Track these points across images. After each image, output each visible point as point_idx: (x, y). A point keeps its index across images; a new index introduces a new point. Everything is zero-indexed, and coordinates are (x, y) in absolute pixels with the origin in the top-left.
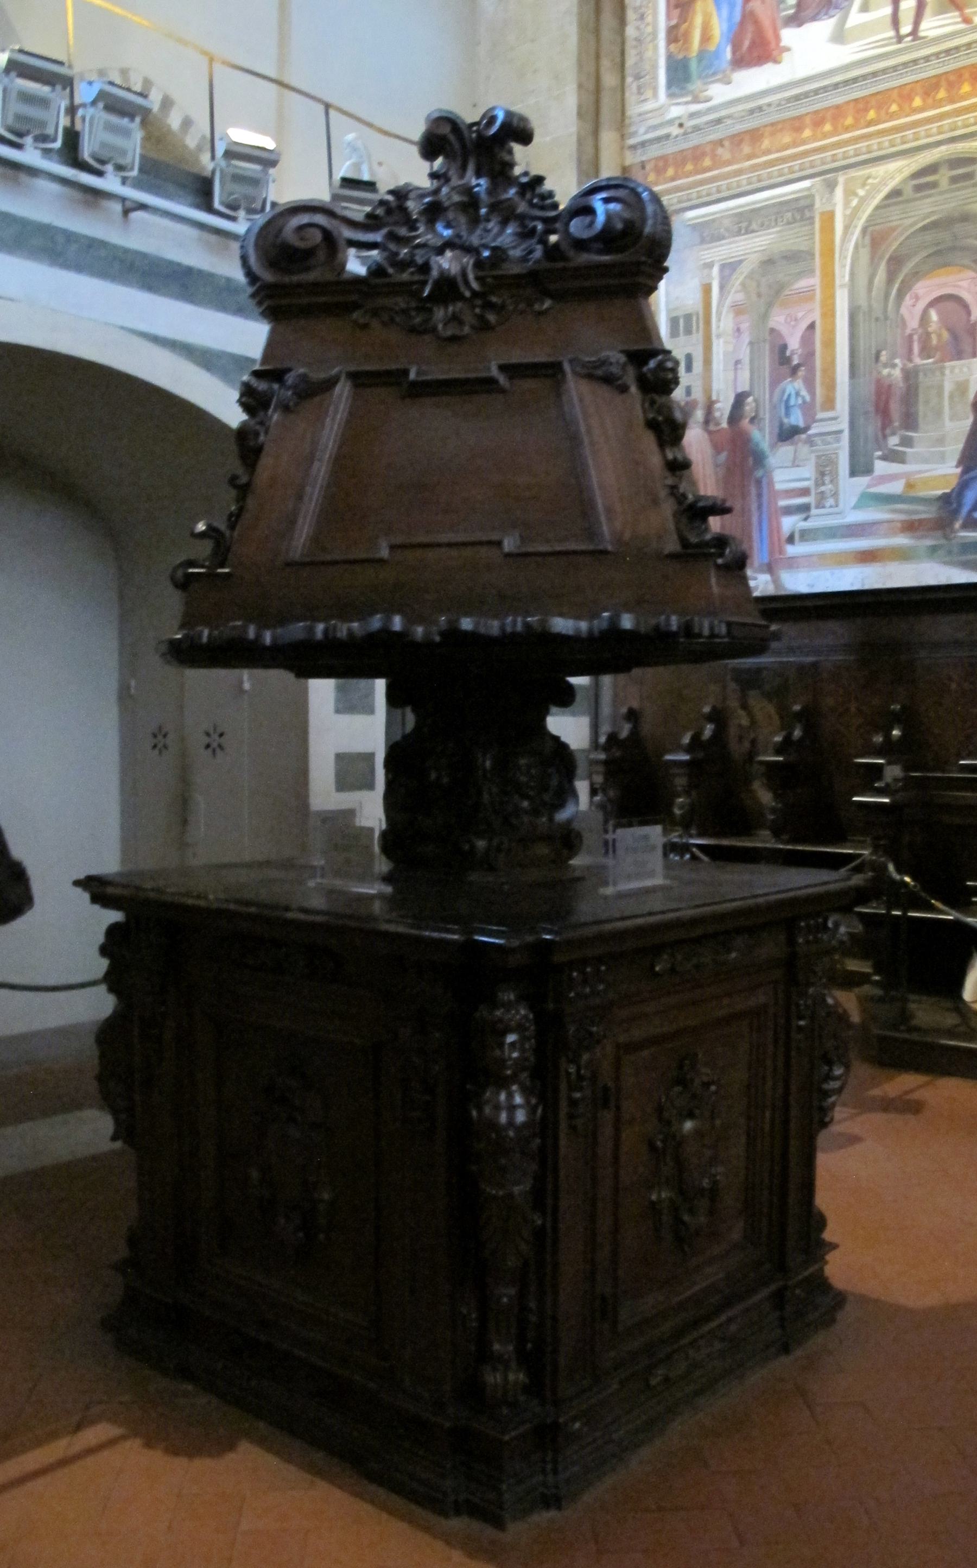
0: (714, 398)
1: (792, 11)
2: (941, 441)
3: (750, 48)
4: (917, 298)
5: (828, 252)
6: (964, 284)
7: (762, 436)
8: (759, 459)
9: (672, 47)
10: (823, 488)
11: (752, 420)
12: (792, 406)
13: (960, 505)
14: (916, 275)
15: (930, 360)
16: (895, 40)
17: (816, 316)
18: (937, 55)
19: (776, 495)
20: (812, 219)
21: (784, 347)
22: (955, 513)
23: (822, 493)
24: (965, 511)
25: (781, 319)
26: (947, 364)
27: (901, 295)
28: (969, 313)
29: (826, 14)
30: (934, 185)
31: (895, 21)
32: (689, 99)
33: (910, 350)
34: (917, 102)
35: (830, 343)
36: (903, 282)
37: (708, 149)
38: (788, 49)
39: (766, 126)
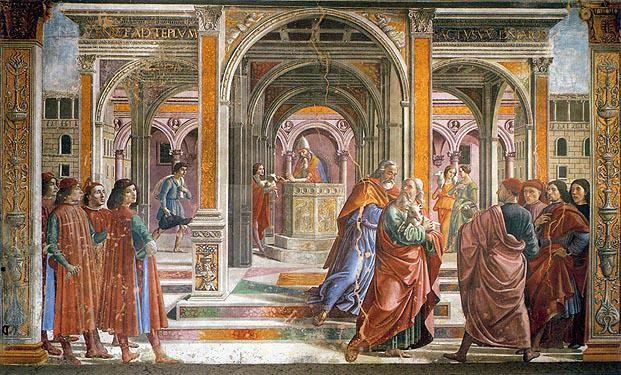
7: (143, 222)
10: (204, 273)
11: (133, 206)
14: (291, 107)
15: (304, 180)
17: (198, 124)
19: (155, 276)
21: (167, 146)
25: (164, 121)
27: (277, 121)
28: (337, 148)
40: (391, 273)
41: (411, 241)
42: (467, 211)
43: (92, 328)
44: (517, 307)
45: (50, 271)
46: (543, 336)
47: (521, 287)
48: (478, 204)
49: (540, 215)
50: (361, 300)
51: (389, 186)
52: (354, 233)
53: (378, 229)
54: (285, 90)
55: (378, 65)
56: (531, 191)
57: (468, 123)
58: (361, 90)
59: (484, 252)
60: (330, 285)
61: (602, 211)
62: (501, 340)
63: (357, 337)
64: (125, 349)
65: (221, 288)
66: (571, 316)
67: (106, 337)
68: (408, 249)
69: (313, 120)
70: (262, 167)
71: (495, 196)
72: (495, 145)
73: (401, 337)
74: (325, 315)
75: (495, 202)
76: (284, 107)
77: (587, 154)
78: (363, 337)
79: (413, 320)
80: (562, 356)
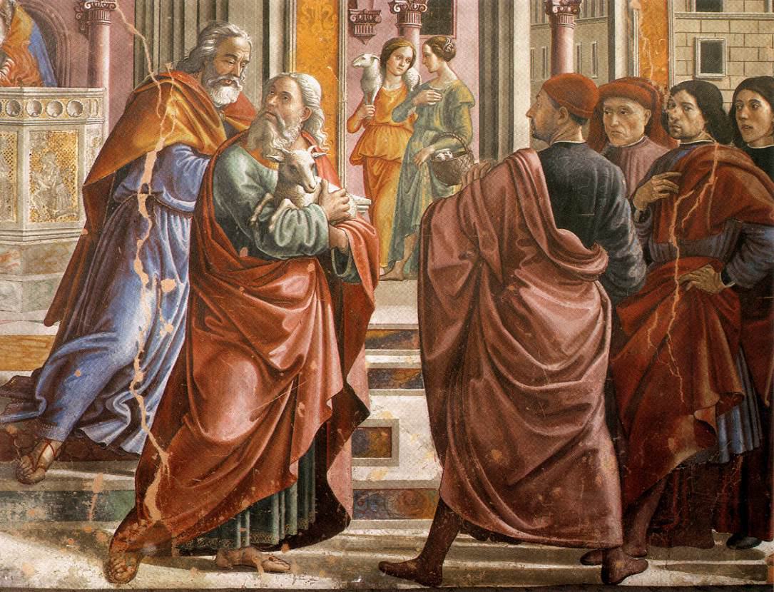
40: (232, 337)
41: (287, 249)
42: (445, 165)
44: (585, 433)
46: (657, 511)
47: (594, 378)
48: (475, 147)
49: (648, 177)
50: (148, 412)
51: (227, 95)
52: (130, 223)
53: (197, 217)
56: (624, 112)
59: (492, 275)
60: (63, 369)
62: (541, 523)
63: (138, 513)
66: (733, 456)
68: (282, 270)
71: (522, 124)
73: (261, 516)
74: (48, 453)
75: (522, 139)
78: (155, 515)
79: (294, 468)
80: (710, 569)
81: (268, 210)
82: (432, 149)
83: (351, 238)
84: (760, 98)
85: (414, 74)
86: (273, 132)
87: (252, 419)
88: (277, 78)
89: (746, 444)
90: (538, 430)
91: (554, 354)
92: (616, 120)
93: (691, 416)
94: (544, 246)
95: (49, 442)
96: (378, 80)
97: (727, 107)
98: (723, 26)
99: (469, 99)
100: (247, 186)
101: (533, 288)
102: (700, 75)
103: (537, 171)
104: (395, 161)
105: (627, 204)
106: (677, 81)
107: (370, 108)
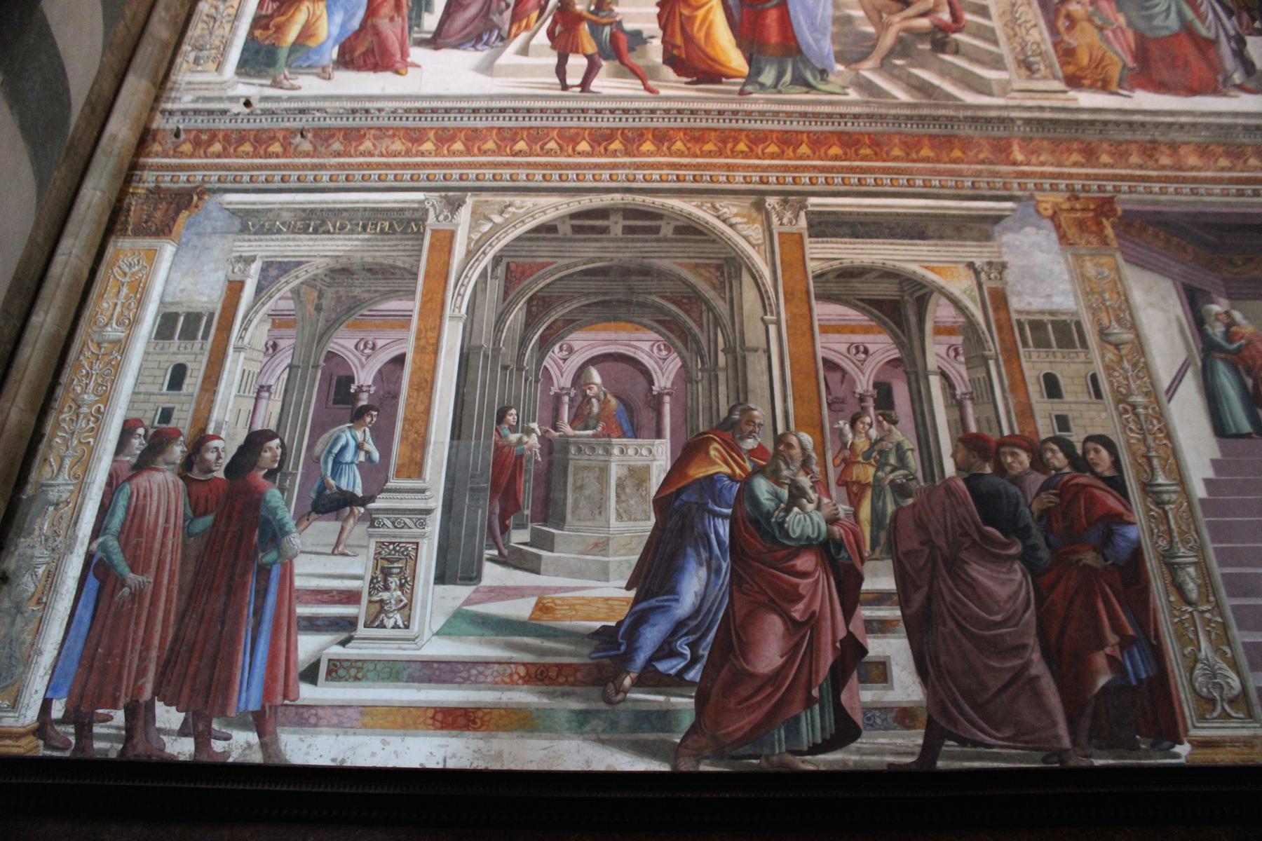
0: (210, 432)
1: (429, 36)
2: (601, 546)
3: (364, 54)
4: (571, 351)
5: (440, 275)
6: (646, 346)
8: (274, 535)
9: (258, 33)
10: (385, 595)
11: (271, 474)
12: (347, 463)
13: (632, 650)
14: (570, 324)
16: (560, 87)
17: (409, 349)
18: (612, 111)
19: (289, 594)
20: (420, 235)
21: (351, 379)
22: (625, 660)
23: (382, 601)
24: (641, 659)
25: (351, 344)
26: (615, 441)
27: (545, 344)
29: (474, 46)
30: (605, 230)
31: (561, 71)
32: (268, 82)
33: (556, 415)
34: (584, 146)
35: (425, 386)
36: (548, 328)
37: (280, 135)
38: (418, 66)
39: (371, 128)
41: (798, 539)
42: (902, 485)
43: (147, 694)
44: (1026, 666)
45: (92, 583)
48: (920, 475)
49: (1038, 494)
51: (750, 444)
54: (562, 299)
55: (719, 267)
56: (1013, 454)
57: (882, 346)
58: (691, 299)
61: (1148, 488)
62: (1008, 732)
64: (203, 740)
65: (415, 626)
66: (1139, 680)
67: (168, 716)
69: (615, 342)
70: (513, 411)
72: (935, 382)
74: (627, 681)
75: (950, 468)
76: (560, 324)
77: (1098, 395)
79: (815, 692)
81: (782, 514)
82: (891, 477)
83: (842, 531)
84: (1100, 447)
85: (874, 433)
86: (783, 466)
87: (782, 657)
88: (783, 435)
89: (1146, 671)
90: (994, 664)
91: (996, 608)
92: (1009, 459)
93: (1102, 652)
94: (976, 537)
95: (628, 673)
96: (850, 436)
97: (1079, 452)
98: (1066, 407)
99: (911, 447)
100: (767, 499)
101: (974, 565)
102: (1058, 433)
103: (965, 493)
104: (868, 484)
105: (1027, 511)
106: (1043, 436)
107: (847, 453)
